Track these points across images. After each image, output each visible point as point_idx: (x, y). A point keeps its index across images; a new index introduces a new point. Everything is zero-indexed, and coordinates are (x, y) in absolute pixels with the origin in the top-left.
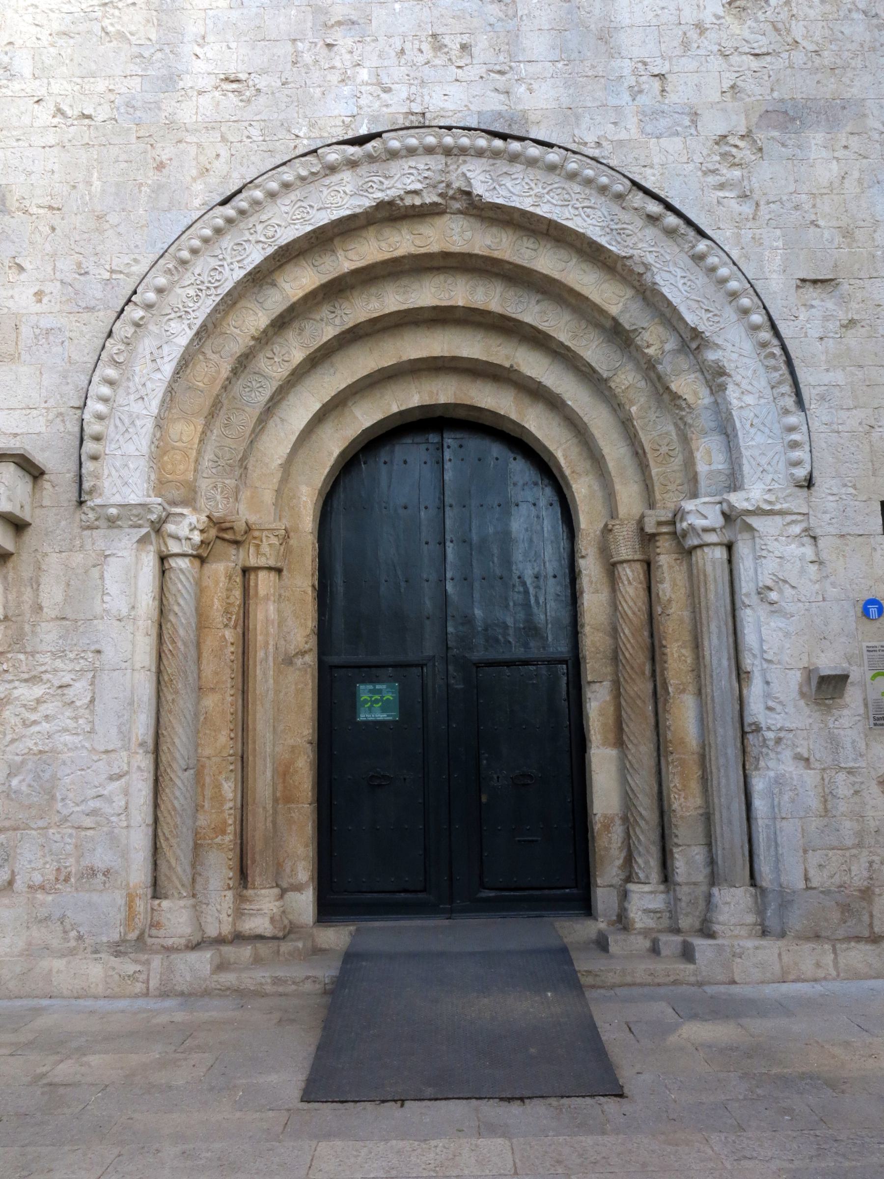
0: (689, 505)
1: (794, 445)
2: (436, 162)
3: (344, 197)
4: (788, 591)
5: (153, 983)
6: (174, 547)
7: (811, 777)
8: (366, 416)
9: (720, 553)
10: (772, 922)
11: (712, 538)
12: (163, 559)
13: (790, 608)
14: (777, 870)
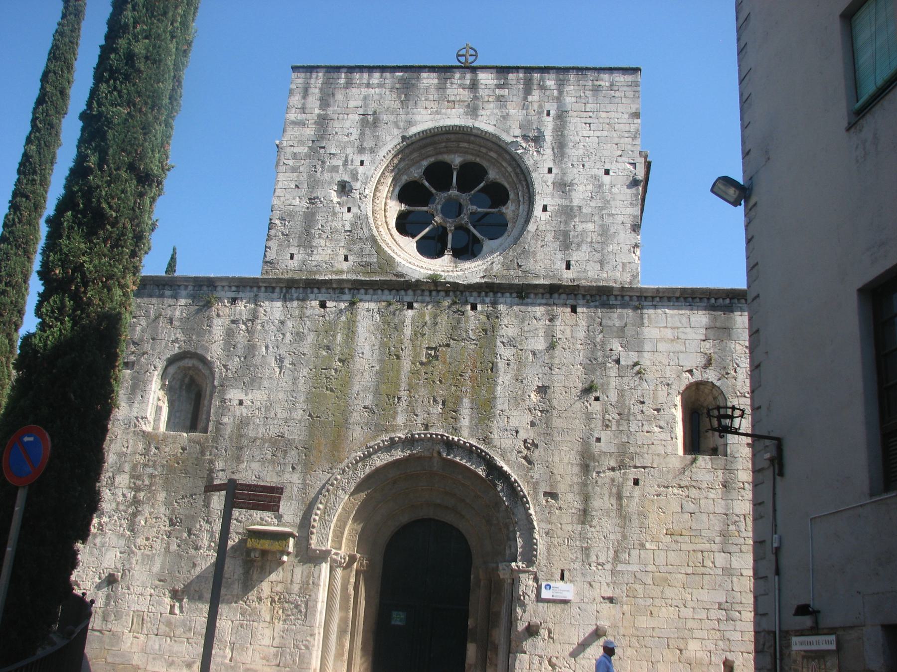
2: (430, 444)
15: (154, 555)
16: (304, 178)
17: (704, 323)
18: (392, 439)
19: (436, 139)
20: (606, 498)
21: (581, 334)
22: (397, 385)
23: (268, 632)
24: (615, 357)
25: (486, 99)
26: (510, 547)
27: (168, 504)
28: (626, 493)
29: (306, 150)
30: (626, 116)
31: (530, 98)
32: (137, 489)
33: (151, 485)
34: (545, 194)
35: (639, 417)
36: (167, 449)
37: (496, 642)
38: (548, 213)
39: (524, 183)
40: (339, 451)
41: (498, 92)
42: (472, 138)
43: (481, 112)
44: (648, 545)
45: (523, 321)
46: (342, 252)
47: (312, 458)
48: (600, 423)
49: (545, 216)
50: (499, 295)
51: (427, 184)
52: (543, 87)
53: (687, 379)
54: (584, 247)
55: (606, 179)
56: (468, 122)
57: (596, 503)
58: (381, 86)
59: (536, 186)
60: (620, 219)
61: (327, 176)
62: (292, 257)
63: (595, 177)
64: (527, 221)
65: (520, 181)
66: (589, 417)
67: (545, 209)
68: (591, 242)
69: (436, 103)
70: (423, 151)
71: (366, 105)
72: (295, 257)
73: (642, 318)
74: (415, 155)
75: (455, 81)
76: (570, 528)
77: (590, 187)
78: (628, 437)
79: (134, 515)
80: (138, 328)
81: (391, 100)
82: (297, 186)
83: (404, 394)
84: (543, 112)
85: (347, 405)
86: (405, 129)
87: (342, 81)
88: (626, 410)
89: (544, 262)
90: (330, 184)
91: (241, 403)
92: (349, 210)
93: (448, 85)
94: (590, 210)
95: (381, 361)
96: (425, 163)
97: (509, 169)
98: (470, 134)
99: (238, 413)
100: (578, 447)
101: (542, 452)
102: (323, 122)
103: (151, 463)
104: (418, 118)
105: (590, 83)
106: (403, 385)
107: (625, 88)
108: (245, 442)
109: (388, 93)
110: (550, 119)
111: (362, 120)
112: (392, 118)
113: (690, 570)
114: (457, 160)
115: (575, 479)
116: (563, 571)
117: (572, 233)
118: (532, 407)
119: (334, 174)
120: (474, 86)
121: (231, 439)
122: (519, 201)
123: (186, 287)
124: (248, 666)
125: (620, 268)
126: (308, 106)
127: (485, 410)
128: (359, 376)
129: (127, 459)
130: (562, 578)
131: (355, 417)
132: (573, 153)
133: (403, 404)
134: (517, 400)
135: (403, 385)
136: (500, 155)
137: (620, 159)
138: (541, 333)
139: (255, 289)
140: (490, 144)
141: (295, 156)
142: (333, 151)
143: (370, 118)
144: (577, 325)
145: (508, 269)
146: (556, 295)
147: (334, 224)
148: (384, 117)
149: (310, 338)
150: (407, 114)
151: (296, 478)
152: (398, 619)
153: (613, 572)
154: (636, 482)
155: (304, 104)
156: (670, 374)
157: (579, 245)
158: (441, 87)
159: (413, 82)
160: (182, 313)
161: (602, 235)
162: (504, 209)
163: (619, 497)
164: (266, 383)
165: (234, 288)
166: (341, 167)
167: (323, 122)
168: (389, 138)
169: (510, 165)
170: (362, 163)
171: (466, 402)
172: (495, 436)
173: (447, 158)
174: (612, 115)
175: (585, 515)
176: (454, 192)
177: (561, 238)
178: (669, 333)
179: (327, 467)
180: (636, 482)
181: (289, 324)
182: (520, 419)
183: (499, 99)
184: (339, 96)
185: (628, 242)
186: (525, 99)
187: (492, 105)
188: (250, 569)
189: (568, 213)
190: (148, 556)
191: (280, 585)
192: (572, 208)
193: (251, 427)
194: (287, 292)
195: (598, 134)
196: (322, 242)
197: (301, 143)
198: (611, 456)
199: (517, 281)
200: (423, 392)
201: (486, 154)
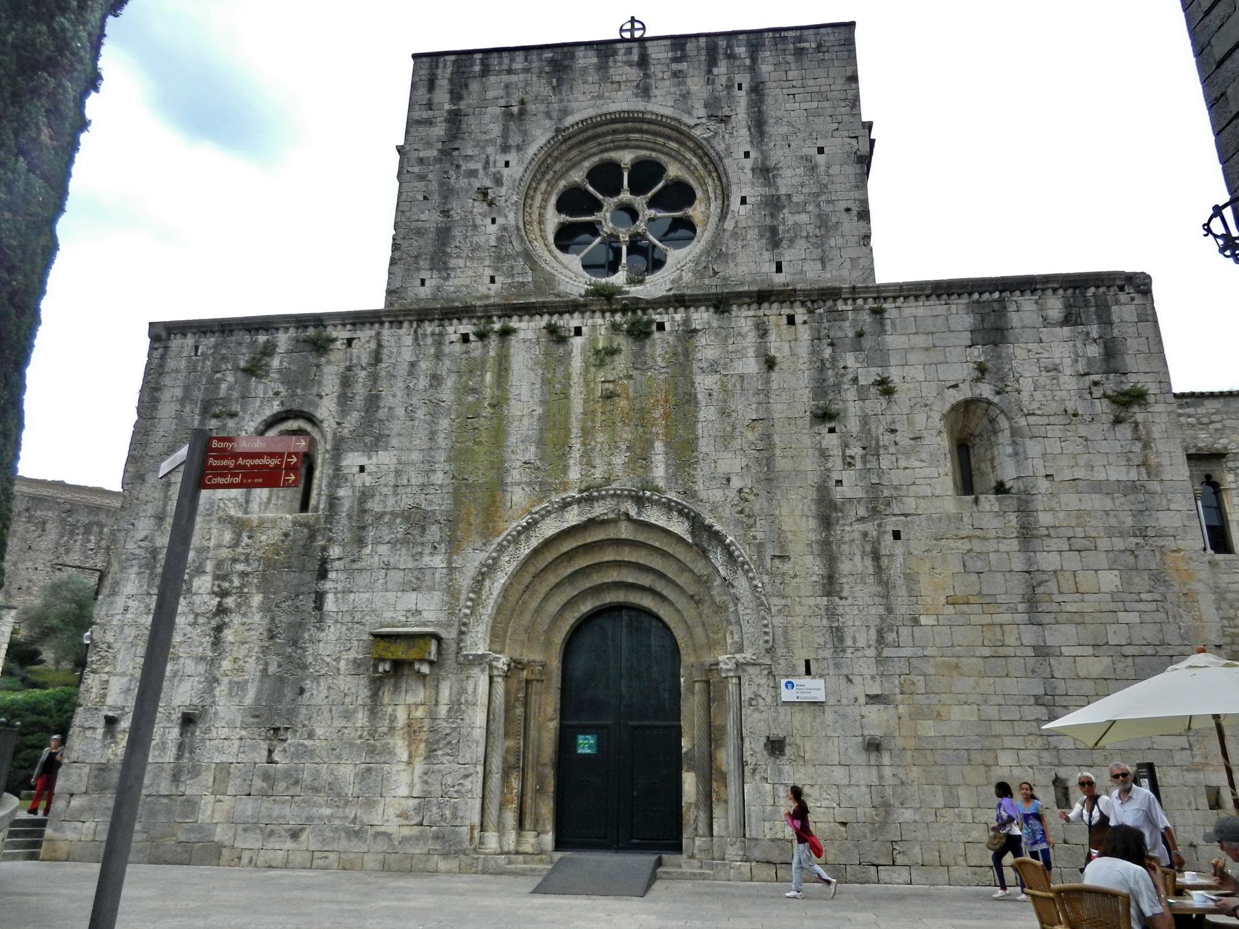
0: (721, 658)
1: (766, 633)
3: (573, 517)
4: (760, 700)
5: (480, 868)
6: (495, 673)
7: (768, 787)
8: (586, 607)
9: (734, 680)
11: (731, 674)
12: (491, 678)
13: (761, 708)
15: (246, 682)
16: (434, 186)
17: (967, 325)
18: (563, 499)
19: (599, 130)
20: (857, 558)
21: (803, 349)
22: (568, 431)
24: (850, 376)
25: (660, 75)
26: (732, 633)
27: (265, 608)
28: (884, 551)
29: (435, 153)
30: (840, 81)
31: (715, 71)
32: (224, 594)
33: (243, 586)
34: (745, 185)
35: (892, 449)
36: (264, 538)
37: (724, 768)
38: (748, 207)
39: (714, 174)
41: (675, 66)
42: (645, 126)
43: (654, 92)
44: (923, 620)
45: (726, 338)
46: (489, 272)
47: (459, 533)
48: (839, 462)
49: (743, 210)
50: (692, 309)
51: (591, 189)
52: (731, 56)
53: (954, 397)
54: (801, 243)
55: (821, 159)
56: (638, 105)
57: (845, 567)
58: (526, 70)
59: (731, 174)
60: (842, 205)
61: (463, 182)
62: (423, 282)
63: (808, 159)
64: (723, 216)
65: (710, 173)
66: (824, 454)
67: (744, 201)
68: (807, 237)
69: (597, 86)
70: (584, 148)
71: (508, 94)
72: (427, 283)
73: (882, 324)
74: (574, 152)
75: (619, 58)
76: (812, 601)
77: (800, 171)
78: (880, 478)
79: (219, 629)
80: (224, 386)
81: (541, 87)
82: (425, 198)
83: (576, 444)
84: (733, 86)
85: (503, 461)
86: (560, 120)
87: (477, 68)
88: (874, 442)
89: (750, 265)
90: (467, 191)
91: (362, 469)
92: (493, 221)
93: (611, 64)
94: (802, 198)
95: (543, 402)
96: (587, 164)
97: (695, 161)
98: (643, 121)
99: (358, 483)
100: (812, 494)
101: (765, 504)
102: (455, 118)
103: (242, 558)
104: (575, 105)
105: (791, 46)
106: (575, 430)
107: (836, 49)
108: (369, 519)
109: (535, 79)
110: (743, 93)
111: (504, 113)
112: (542, 107)
113: (987, 652)
114: (626, 158)
115: (813, 537)
116: (807, 663)
117: (781, 228)
118: (745, 446)
119: (472, 180)
120: (643, 62)
121: (350, 517)
122: (709, 199)
123: (287, 329)
124: (379, 829)
125: (847, 264)
126: (436, 101)
127: (684, 454)
128: (516, 423)
129: (210, 555)
130: (808, 672)
131: (515, 475)
132: (775, 131)
133: (576, 454)
134: (725, 440)
135: (574, 431)
136: (682, 144)
137: (836, 133)
138: (751, 352)
139: (377, 326)
140: (667, 131)
141: (421, 161)
142: (470, 152)
143: (515, 110)
144: (796, 340)
145: (702, 276)
146: (766, 305)
147: (475, 239)
148: (531, 107)
149: (450, 382)
150: (561, 101)
151: (438, 561)
152: (586, 745)
153: (880, 660)
154: (897, 535)
155: (430, 99)
156: (929, 391)
157: (792, 241)
158: (603, 67)
159: (566, 63)
160: (281, 363)
161: (820, 228)
162: (690, 211)
163: (876, 556)
164: (394, 442)
165: (349, 327)
166: (481, 171)
167: (455, 118)
168: (538, 132)
169: (695, 155)
170: (507, 164)
171: (659, 446)
172: (699, 487)
173: (614, 155)
174: (822, 81)
175: (830, 585)
176: (625, 196)
177: (768, 234)
178: (921, 341)
179: (478, 544)
180: (897, 535)
181: (424, 365)
182: (731, 463)
183: (675, 74)
184: (474, 86)
185: (856, 233)
186: (709, 72)
187: (667, 83)
188: (379, 689)
189: (773, 204)
190: (237, 683)
191: (421, 708)
192: (779, 198)
193: (377, 498)
194: (419, 326)
195: (806, 105)
196: (461, 262)
197: (429, 144)
198: (859, 502)
199: (713, 291)
200: (601, 437)
201: (664, 145)
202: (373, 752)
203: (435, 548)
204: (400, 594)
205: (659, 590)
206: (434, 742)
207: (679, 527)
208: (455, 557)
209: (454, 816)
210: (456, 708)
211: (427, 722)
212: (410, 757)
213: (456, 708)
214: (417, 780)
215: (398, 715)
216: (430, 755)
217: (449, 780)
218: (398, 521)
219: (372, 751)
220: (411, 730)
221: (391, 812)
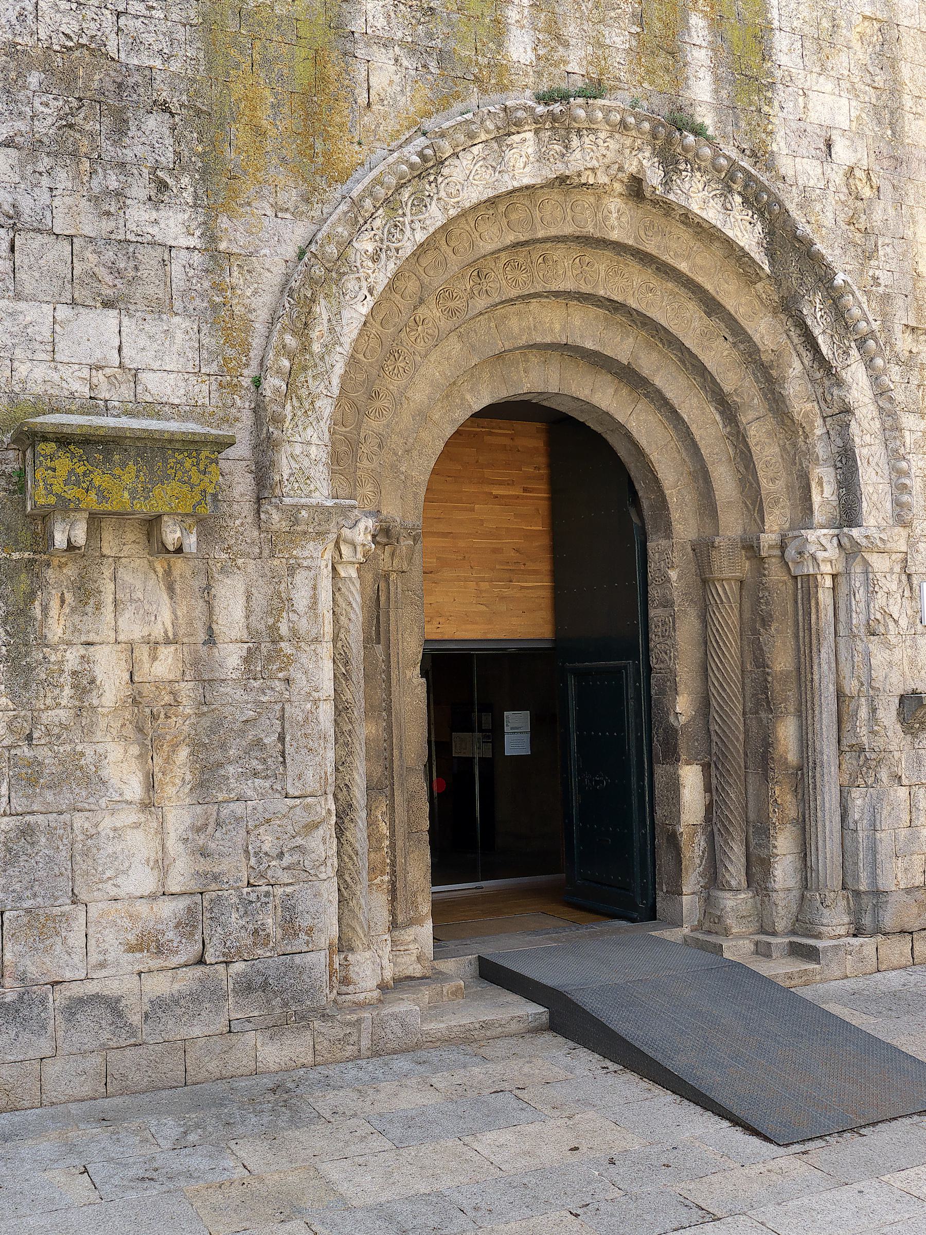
5: (365, 1043)
7: (902, 792)
10: (867, 920)
14: (874, 876)
23: (140, 843)
26: (820, 483)
40: (327, 137)
101: (891, 211)
151: (175, 226)
172: (779, 146)
179: (290, 197)
188: (31, 596)
191: (167, 653)
202: (32, 782)
203: (163, 186)
204: (63, 312)
205: (645, 373)
206: (210, 743)
207: (746, 233)
208: (224, 222)
209: (290, 926)
210: (267, 652)
211: (186, 689)
212: (150, 785)
213: (267, 652)
214: (174, 846)
215: (99, 672)
216: (206, 780)
217: (268, 844)
218: (34, 79)
219: (30, 777)
220: (145, 718)
221: (111, 942)
